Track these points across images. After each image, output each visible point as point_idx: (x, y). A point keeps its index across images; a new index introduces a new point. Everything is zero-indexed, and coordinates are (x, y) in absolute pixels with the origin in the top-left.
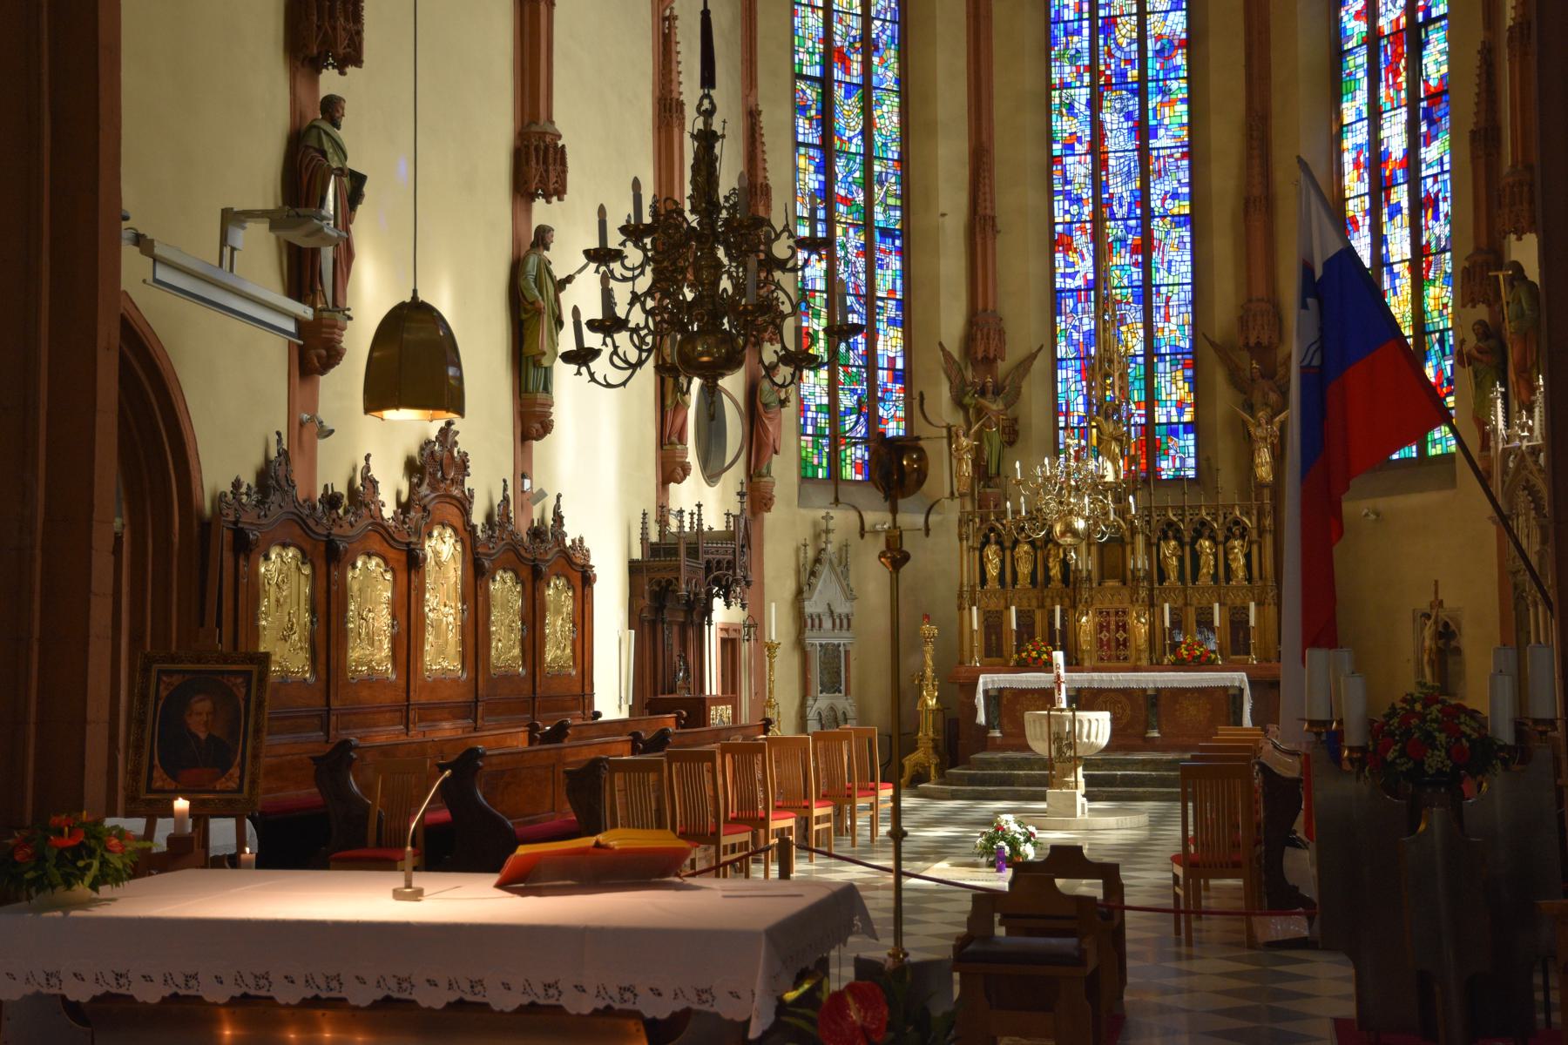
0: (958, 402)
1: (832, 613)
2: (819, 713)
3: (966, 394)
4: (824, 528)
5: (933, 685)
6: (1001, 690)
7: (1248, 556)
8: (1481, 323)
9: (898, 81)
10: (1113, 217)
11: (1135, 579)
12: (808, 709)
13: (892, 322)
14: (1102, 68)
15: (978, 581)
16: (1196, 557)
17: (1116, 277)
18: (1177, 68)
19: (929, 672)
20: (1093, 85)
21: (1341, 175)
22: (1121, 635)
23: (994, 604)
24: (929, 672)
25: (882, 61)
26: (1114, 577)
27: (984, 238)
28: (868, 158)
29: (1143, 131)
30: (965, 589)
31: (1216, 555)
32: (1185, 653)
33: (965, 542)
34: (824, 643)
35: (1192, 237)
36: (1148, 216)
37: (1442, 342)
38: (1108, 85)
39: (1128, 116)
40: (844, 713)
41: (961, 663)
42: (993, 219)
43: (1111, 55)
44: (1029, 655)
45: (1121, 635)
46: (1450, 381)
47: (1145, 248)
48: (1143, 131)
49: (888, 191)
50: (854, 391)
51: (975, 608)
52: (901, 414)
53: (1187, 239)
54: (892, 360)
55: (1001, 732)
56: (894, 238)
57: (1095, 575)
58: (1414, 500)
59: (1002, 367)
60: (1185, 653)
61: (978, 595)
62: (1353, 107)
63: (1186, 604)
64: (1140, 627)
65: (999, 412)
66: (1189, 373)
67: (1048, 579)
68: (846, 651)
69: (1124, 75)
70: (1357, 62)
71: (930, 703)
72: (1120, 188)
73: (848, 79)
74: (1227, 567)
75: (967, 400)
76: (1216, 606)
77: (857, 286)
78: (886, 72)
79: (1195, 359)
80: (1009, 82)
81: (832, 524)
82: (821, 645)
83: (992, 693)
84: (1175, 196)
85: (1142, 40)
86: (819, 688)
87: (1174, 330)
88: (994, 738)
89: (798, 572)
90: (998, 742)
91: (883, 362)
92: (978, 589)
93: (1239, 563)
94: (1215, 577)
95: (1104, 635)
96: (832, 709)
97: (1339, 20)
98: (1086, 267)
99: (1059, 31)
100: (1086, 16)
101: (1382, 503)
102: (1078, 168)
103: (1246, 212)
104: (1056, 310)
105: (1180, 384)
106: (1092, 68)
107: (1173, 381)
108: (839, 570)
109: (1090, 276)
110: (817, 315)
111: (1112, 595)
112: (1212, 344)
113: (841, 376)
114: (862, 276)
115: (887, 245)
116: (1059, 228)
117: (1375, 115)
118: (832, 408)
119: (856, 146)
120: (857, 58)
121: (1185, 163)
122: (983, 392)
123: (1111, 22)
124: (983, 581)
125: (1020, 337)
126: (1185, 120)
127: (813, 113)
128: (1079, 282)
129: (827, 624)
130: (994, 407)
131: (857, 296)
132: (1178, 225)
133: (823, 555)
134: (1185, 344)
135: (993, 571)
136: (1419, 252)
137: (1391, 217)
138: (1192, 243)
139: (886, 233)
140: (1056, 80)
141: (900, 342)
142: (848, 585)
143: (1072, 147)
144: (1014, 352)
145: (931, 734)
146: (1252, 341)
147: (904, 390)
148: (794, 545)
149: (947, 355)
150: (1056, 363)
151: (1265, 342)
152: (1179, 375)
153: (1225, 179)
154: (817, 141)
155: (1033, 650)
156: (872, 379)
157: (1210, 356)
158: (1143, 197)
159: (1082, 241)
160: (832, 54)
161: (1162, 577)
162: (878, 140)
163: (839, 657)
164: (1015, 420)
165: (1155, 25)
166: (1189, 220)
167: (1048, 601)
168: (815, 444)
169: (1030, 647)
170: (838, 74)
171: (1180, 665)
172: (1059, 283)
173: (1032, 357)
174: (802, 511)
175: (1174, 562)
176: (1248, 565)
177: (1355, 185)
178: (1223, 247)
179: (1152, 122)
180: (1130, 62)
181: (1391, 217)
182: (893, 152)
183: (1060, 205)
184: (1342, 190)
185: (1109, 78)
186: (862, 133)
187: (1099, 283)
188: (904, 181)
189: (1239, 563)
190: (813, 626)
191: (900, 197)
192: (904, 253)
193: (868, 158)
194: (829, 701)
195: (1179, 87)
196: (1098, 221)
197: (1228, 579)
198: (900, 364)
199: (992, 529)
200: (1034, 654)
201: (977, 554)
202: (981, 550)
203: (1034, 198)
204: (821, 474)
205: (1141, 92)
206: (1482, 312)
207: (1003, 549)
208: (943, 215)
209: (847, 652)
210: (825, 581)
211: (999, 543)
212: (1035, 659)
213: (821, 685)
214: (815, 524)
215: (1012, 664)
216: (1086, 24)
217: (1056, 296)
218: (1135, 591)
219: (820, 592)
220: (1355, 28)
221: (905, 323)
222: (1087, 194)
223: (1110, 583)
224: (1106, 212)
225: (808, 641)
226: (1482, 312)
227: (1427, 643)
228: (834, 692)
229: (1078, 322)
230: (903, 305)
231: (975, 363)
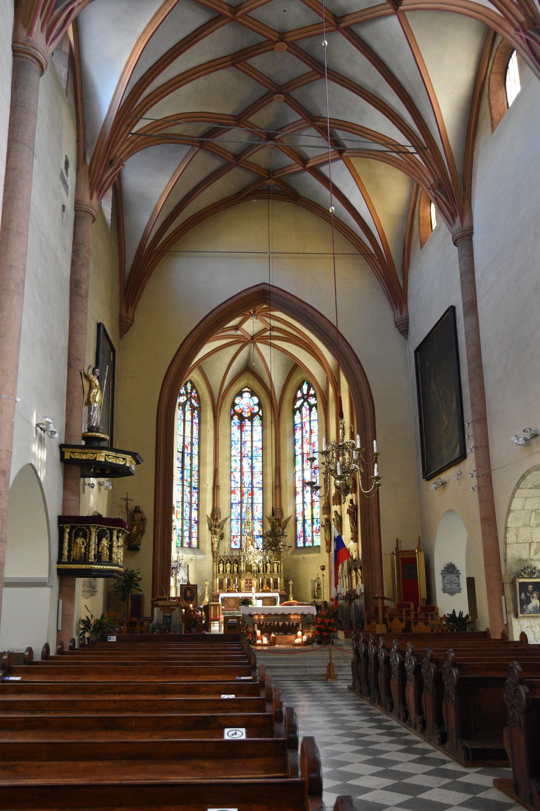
0: (210, 529)
3: (212, 527)
6: (224, 597)
7: (278, 567)
8: (326, 518)
9: (198, 453)
10: (245, 487)
11: (254, 572)
13: (195, 509)
14: (243, 452)
16: (266, 567)
17: (245, 501)
18: (259, 454)
19: (207, 593)
20: (241, 456)
21: (295, 482)
22: (250, 585)
23: (221, 577)
24: (207, 593)
25: (195, 448)
26: (249, 571)
27: (217, 491)
28: (191, 470)
29: (252, 467)
31: (271, 567)
32: (265, 589)
35: (263, 492)
36: (252, 487)
37: (317, 521)
38: (244, 456)
39: (249, 464)
41: (213, 591)
42: (219, 486)
43: (245, 450)
45: (250, 585)
46: (319, 530)
47: (252, 494)
48: (252, 467)
49: (195, 478)
50: (186, 526)
51: (218, 578)
52: (196, 531)
53: (262, 493)
54: (195, 518)
56: (196, 489)
57: (245, 571)
58: (311, 555)
59: (220, 521)
60: (265, 589)
62: (298, 467)
63: (264, 578)
64: (255, 582)
65: (219, 532)
66: (261, 524)
67: (234, 572)
69: (248, 455)
70: (299, 458)
72: (247, 479)
73: (187, 452)
74: (273, 569)
75: (212, 529)
76: (271, 578)
77: (188, 501)
78: (195, 451)
79: (263, 521)
80: (223, 454)
84: (259, 483)
85: (252, 447)
87: (258, 514)
91: (193, 519)
93: (276, 569)
94: (270, 572)
95: (247, 585)
97: (295, 448)
98: (238, 499)
99: (233, 443)
100: (240, 440)
101: (305, 556)
102: (237, 475)
103: (275, 489)
104: (231, 508)
105: (259, 526)
106: (241, 452)
107: (258, 525)
109: (240, 500)
110: (179, 507)
111: (249, 575)
112: (267, 518)
113: (184, 522)
114: (189, 498)
115: (194, 491)
116: (232, 489)
117: (303, 470)
118: (182, 530)
119: (189, 468)
120: (189, 447)
121: (261, 475)
122: (215, 527)
123: (245, 442)
125: (224, 514)
126: (261, 466)
127: (180, 460)
128: (237, 502)
130: (218, 530)
131: (188, 503)
132: (259, 490)
133: (181, 565)
134: (261, 517)
135: (221, 569)
136: (312, 502)
137: (306, 492)
138: (263, 494)
139: (195, 488)
140: (232, 454)
141: (197, 514)
143: (236, 470)
144: (223, 517)
146: (277, 518)
147: (197, 525)
150: (231, 520)
151: (279, 518)
152: (259, 524)
153: (270, 481)
154: (181, 466)
156: (190, 523)
157: (266, 520)
158: (252, 483)
159: (238, 492)
160: (184, 447)
161: (259, 572)
162: (193, 466)
164: (223, 534)
165: (255, 444)
166: (262, 488)
167: (234, 577)
168: (178, 539)
170: (186, 451)
171: (264, 591)
172: (232, 501)
173: (227, 519)
175: (262, 568)
176: (278, 569)
177: (299, 485)
178: (269, 496)
179: (254, 466)
180: (249, 452)
181: (306, 492)
182: (196, 469)
183: (233, 483)
184: (295, 485)
185: (244, 455)
186: (190, 465)
187: (241, 502)
188: (199, 476)
189: (276, 569)
191: (198, 480)
192: (198, 493)
193: (191, 470)
195: (260, 459)
196: (241, 487)
197: (273, 573)
198: (196, 519)
199: (221, 560)
202: (219, 564)
203: (228, 481)
204: (179, 545)
205: (252, 459)
206: (326, 516)
207: (224, 564)
211: (223, 563)
216: (239, 442)
217: (232, 504)
218: (254, 574)
220: (298, 451)
221: (198, 510)
222: (239, 481)
223: (249, 573)
224: (243, 486)
226: (326, 516)
227: (316, 586)
229: (236, 510)
230: (198, 505)
231: (214, 519)
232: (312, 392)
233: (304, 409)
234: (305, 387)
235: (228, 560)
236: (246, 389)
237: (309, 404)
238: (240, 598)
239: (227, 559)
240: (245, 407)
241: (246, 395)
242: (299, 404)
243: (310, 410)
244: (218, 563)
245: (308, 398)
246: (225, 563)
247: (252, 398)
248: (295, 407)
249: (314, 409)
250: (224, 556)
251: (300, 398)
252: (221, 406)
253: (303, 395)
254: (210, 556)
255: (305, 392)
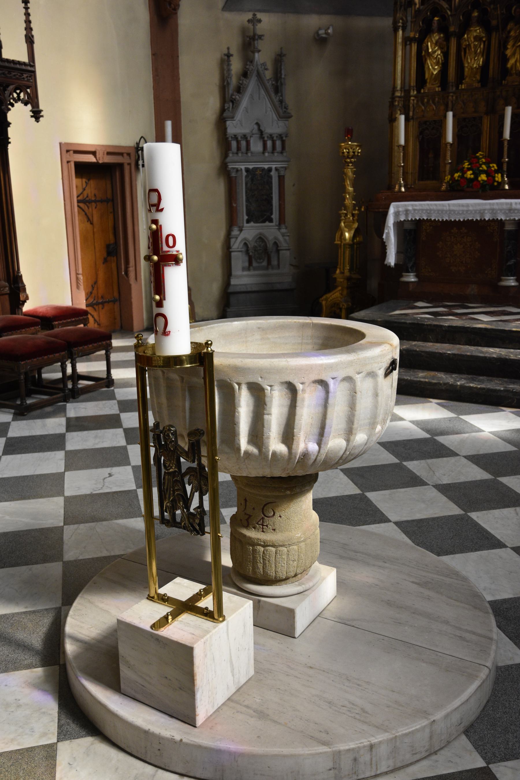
1: (261, 132)
2: (245, 244)
4: (251, 34)
5: (353, 215)
6: (419, 222)
12: (233, 241)
15: (413, 83)
30: (398, 94)
33: (400, 32)
34: (251, 167)
40: (276, 244)
44: (462, 177)
55: (417, 276)
68: (279, 177)
71: (347, 235)
81: (260, 28)
82: (247, 170)
83: (407, 226)
86: (246, 217)
88: (408, 283)
89: (224, 87)
90: (411, 287)
92: (414, 93)
96: (261, 239)
108: (269, 85)
124: (421, 81)
129: (256, 146)
142: (281, 102)
145: (347, 273)
148: (217, 56)
155: (469, 169)
163: (270, 183)
169: (466, 165)
174: (228, 15)
190: (239, 148)
194: (258, 231)
200: (469, 174)
201: (415, 47)
202: (421, 42)
207: (447, 39)
209: (281, 179)
210: (252, 97)
211: (443, 29)
212: (470, 180)
213: (248, 214)
214: (244, 31)
215: (444, 188)
219: (246, 110)
225: (231, 166)
228: (264, 222)
238: (509, 227)
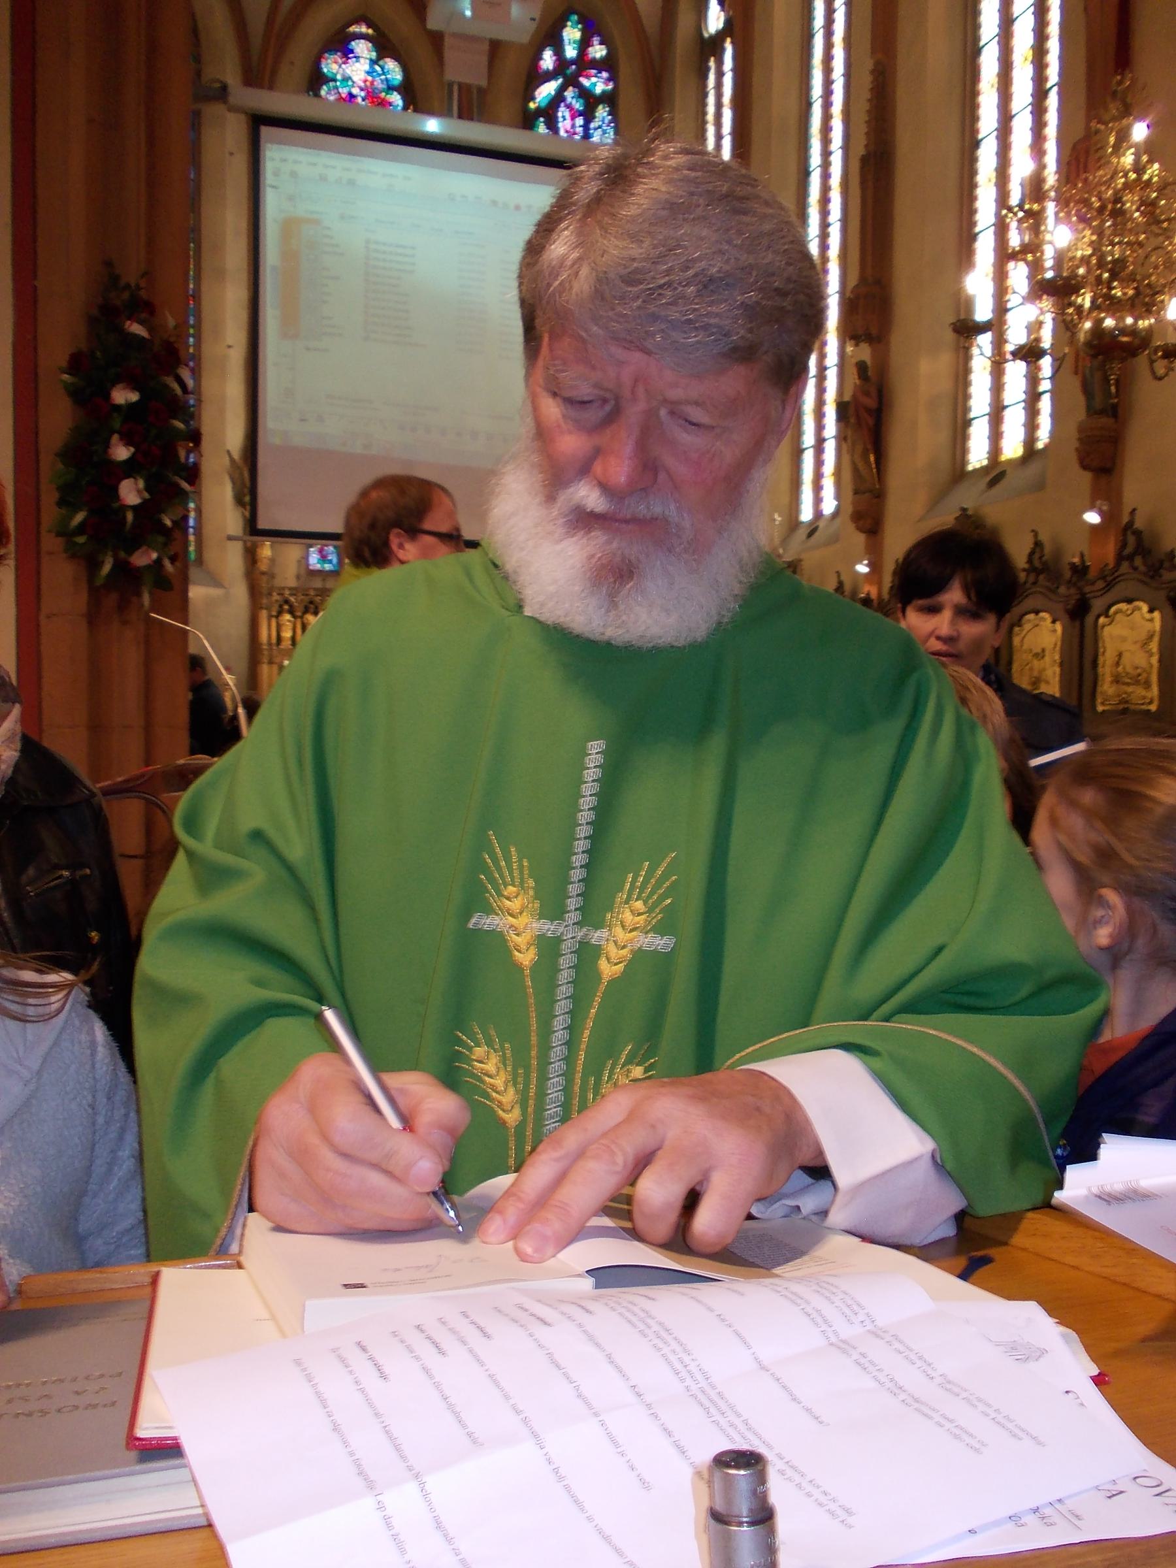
61: (275, 653)
149: (232, 460)
199: (287, 602)
202: (277, 617)
208: (229, 347)
232: (598, 51)
233: (563, 112)
234: (572, 34)
235: (311, 602)
236: (364, 29)
237: (585, 94)
239: (307, 599)
240: (355, 91)
241: (362, 48)
242: (547, 90)
243: (588, 115)
244: (274, 613)
245: (579, 73)
246: (299, 614)
247: (381, 63)
248: (532, 105)
249: (602, 112)
250: (294, 591)
251: (548, 76)
252: (274, 73)
253: (562, 63)
254: (240, 592)
255: (571, 52)
